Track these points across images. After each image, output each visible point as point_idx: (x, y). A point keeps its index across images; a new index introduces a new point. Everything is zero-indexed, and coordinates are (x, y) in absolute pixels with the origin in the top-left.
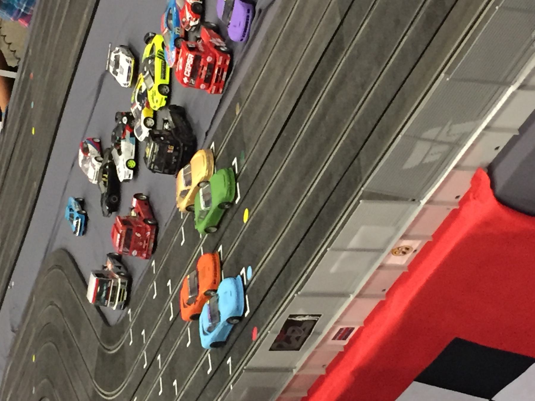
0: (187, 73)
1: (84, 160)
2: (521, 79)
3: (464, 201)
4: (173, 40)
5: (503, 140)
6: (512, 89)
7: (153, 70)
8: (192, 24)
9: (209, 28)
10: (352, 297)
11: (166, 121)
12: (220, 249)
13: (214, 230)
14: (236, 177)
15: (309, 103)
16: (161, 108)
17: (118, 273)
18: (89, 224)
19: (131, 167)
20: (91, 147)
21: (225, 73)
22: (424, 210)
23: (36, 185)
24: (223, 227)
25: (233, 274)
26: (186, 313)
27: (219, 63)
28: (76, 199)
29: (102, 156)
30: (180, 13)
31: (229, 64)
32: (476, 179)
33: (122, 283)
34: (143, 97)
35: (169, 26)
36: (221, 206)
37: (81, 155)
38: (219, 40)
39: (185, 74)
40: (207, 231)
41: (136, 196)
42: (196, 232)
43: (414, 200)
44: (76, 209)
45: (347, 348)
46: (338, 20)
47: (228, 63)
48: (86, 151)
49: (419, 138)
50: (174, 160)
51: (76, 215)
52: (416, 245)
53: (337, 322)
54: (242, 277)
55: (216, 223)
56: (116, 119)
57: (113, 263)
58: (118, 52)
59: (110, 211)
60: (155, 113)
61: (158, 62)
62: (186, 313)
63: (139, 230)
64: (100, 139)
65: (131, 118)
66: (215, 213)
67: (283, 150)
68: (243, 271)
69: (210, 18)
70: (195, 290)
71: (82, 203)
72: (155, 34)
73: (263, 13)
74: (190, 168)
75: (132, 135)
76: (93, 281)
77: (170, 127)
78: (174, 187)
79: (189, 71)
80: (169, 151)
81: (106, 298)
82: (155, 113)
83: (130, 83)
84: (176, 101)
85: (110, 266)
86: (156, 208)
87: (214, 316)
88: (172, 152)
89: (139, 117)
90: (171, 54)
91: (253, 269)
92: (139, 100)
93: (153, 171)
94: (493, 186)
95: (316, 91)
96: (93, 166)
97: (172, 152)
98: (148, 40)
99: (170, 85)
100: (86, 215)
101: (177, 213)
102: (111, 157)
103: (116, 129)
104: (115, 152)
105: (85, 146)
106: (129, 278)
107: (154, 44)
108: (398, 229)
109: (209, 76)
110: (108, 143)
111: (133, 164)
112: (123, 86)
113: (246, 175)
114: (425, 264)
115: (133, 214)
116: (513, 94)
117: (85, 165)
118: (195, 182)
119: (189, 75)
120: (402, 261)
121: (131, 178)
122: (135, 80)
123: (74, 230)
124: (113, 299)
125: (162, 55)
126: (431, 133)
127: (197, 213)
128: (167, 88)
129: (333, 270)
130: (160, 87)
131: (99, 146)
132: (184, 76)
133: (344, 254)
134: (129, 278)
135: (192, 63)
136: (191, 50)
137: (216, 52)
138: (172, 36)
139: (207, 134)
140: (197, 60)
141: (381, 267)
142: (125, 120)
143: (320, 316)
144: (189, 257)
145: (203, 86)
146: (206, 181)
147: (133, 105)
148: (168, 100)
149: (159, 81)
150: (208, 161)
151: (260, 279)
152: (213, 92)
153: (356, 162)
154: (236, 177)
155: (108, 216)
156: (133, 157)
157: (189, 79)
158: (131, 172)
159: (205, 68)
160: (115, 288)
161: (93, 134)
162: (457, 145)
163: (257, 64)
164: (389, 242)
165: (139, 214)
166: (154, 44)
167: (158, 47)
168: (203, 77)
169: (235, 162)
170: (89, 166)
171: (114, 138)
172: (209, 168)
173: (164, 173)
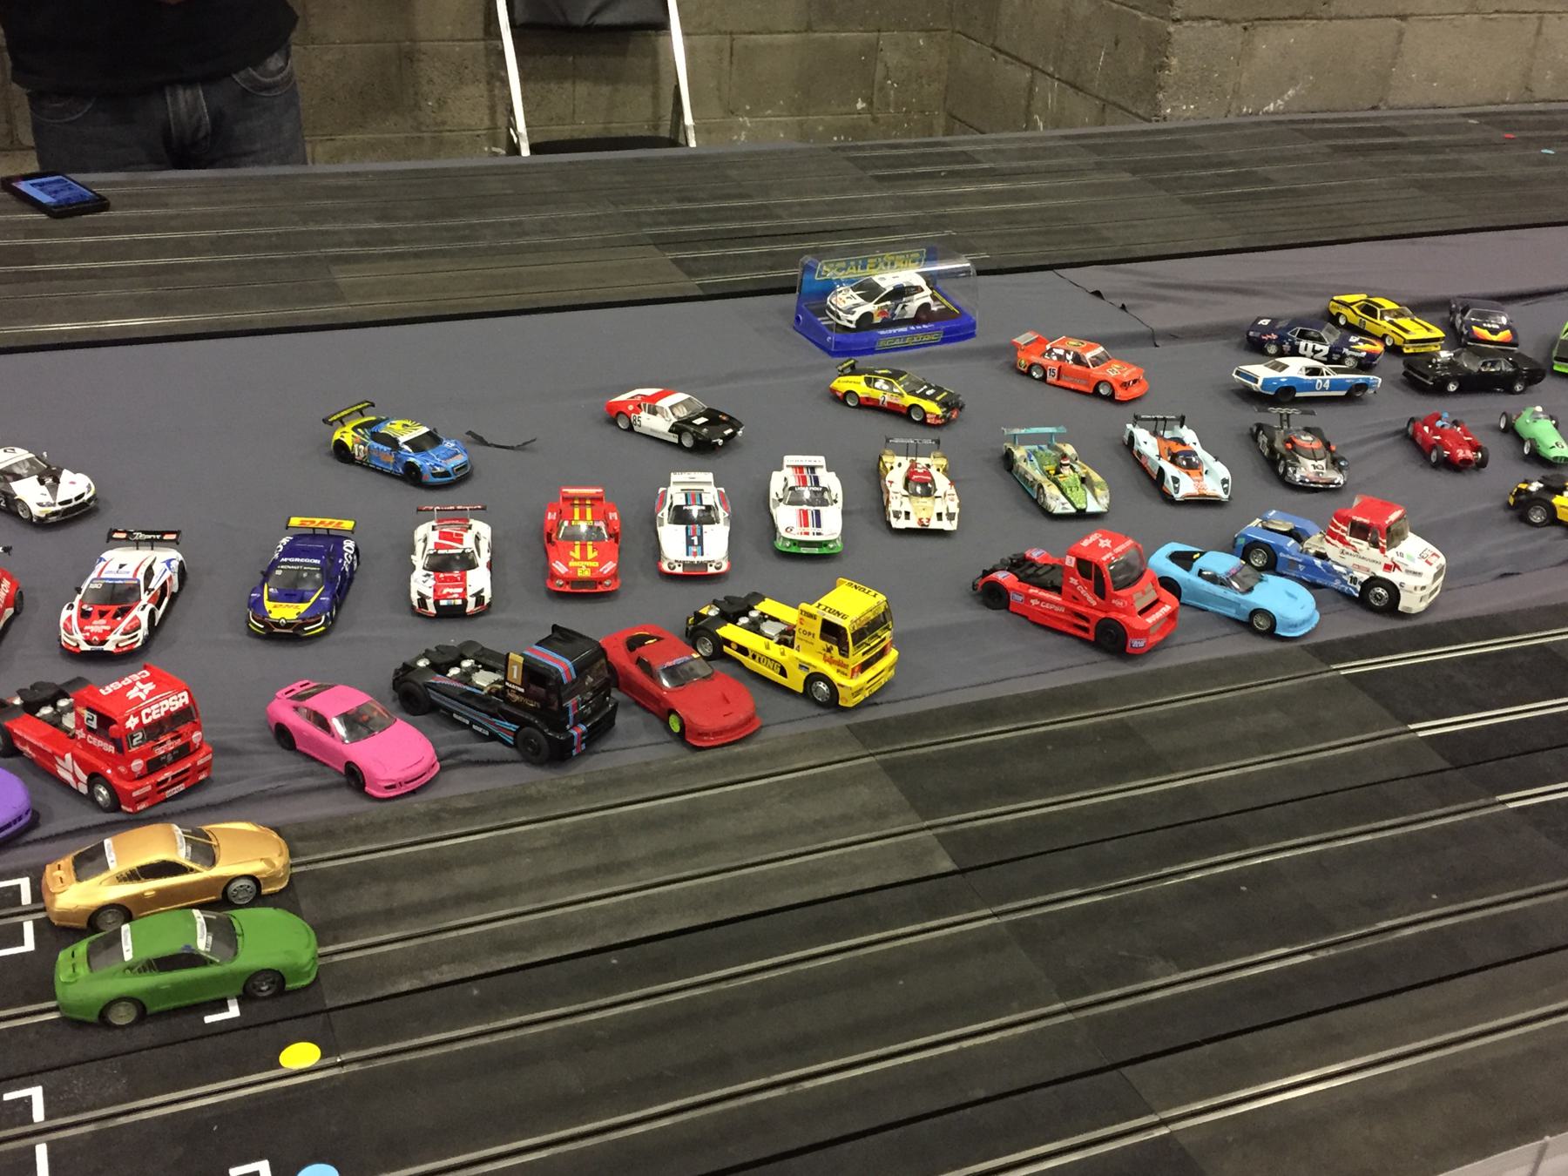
0: (148, 715)
21: (181, 787)
31: (202, 781)
79: (155, 716)
109: (165, 761)
119: (146, 721)
135: (172, 709)
157: (140, 725)
159: (179, 742)
168: (160, 751)
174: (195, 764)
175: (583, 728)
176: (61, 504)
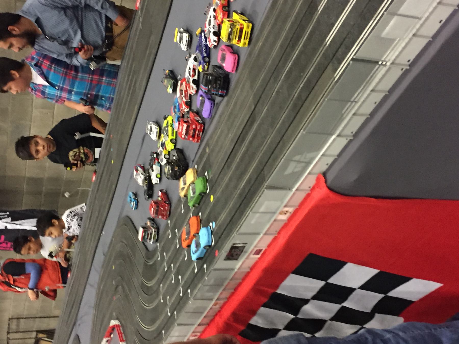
1: (137, 175)
2: (338, 132)
3: (313, 189)
4: (177, 118)
5: (330, 160)
6: (334, 137)
7: (168, 132)
8: (186, 110)
9: (193, 112)
10: (261, 235)
11: (174, 156)
12: (200, 214)
13: (197, 205)
14: (207, 181)
15: (240, 145)
16: (172, 150)
17: (153, 227)
18: (139, 204)
19: (158, 177)
20: (139, 169)
21: (201, 133)
22: (294, 194)
23: (114, 187)
24: (201, 203)
25: (206, 225)
26: (184, 244)
27: (199, 128)
28: (133, 193)
29: (145, 172)
30: (180, 105)
32: (318, 179)
33: (154, 231)
34: (163, 145)
35: (175, 112)
36: (200, 194)
37: (135, 172)
38: (198, 118)
39: (183, 133)
40: (194, 206)
41: (161, 191)
42: (189, 207)
43: (289, 189)
44: (133, 197)
45: (259, 259)
46: (253, 107)
47: (202, 128)
48: (137, 170)
49: (292, 160)
50: (178, 173)
51: (133, 200)
52: (291, 210)
53: (255, 247)
54: (210, 227)
55: (198, 203)
56: (151, 155)
57: (150, 222)
58: (151, 124)
59: (149, 198)
60: (169, 152)
61: (170, 129)
62: (184, 244)
63: (162, 206)
64: (143, 165)
65: (158, 155)
66: (197, 198)
67: (229, 167)
68: (211, 224)
69: (194, 108)
70: (188, 233)
71: (136, 195)
72: (168, 116)
73: (218, 104)
74: (185, 177)
75: (159, 162)
76: (141, 231)
77: (176, 158)
78: (178, 186)
80: (176, 169)
81: (147, 238)
82: (169, 152)
83: (157, 138)
84: (179, 146)
85: (149, 223)
86: (170, 195)
87: (198, 245)
88: (177, 170)
89: (162, 154)
90: (176, 125)
91: (215, 223)
92: (161, 146)
93: (168, 179)
94: (326, 182)
95: (243, 140)
96: (141, 177)
97: (177, 170)
98: (165, 118)
99: (176, 139)
100: (137, 200)
101: (180, 198)
102: (149, 173)
103: (151, 160)
104: (150, 170)
105: (137, 168)
106: (158, 229)
107: (168, 121)
108: (282, 203)
110: (147, 167)
111: (159, 176)
112: (154, 140)
113: (211, 180)
114: (350, 147)
115: (159, 199)
116: (334, 140)
117: (137, 177)
118: (188, 183)
119: (184, 134)
120: (284, 217)
121: (158, 182)
122: (159, 137)
123: (132, 207)
124: (150, 239)
125: (172, 125)
126: (297, 158)
127: (189, 198)
128: (174, 140)
129: (253, 222)
130: (171, 140)
131: (143, 168)
132: (182, 134)
133: (258, 215)
134: (158, 229)
136: (185, 122)
137: (197, 123)
138: (177, 117)
139: (193, 161)
140: (188, 127)
141: (275, 220)
142: (155, 156)
143: (246, 244)
144: (185, 218)
145: (191, 139)
146: (193, 183)
147: (158, 149)
148: (175, 146)
149: (171, 137)
150: (194, 173)
151: (219, 227)
152: (196, 141)
153: (262, 172)
154: (207, 181)
155: (148, 200)
156: (159, 173)
158: (158, 180)
159: (192, 131)
160: (151, 234)
161: (141, 162)
162: (309, 163)
163: (216, 129)
164: (278, 209)
165: (162, 199)
166: (168, 121)
167: (170, 122)
168: (191, 135)
169: (206, 174)
170: (138, 177)
171: (150, 164)
172: (194, 177)
173: (174, 179)
174: (198, 130)
175: (220, 90)
176: (186, 45)
